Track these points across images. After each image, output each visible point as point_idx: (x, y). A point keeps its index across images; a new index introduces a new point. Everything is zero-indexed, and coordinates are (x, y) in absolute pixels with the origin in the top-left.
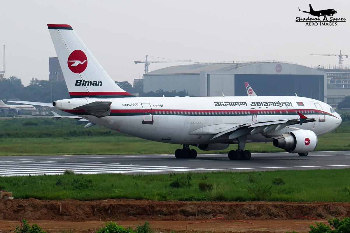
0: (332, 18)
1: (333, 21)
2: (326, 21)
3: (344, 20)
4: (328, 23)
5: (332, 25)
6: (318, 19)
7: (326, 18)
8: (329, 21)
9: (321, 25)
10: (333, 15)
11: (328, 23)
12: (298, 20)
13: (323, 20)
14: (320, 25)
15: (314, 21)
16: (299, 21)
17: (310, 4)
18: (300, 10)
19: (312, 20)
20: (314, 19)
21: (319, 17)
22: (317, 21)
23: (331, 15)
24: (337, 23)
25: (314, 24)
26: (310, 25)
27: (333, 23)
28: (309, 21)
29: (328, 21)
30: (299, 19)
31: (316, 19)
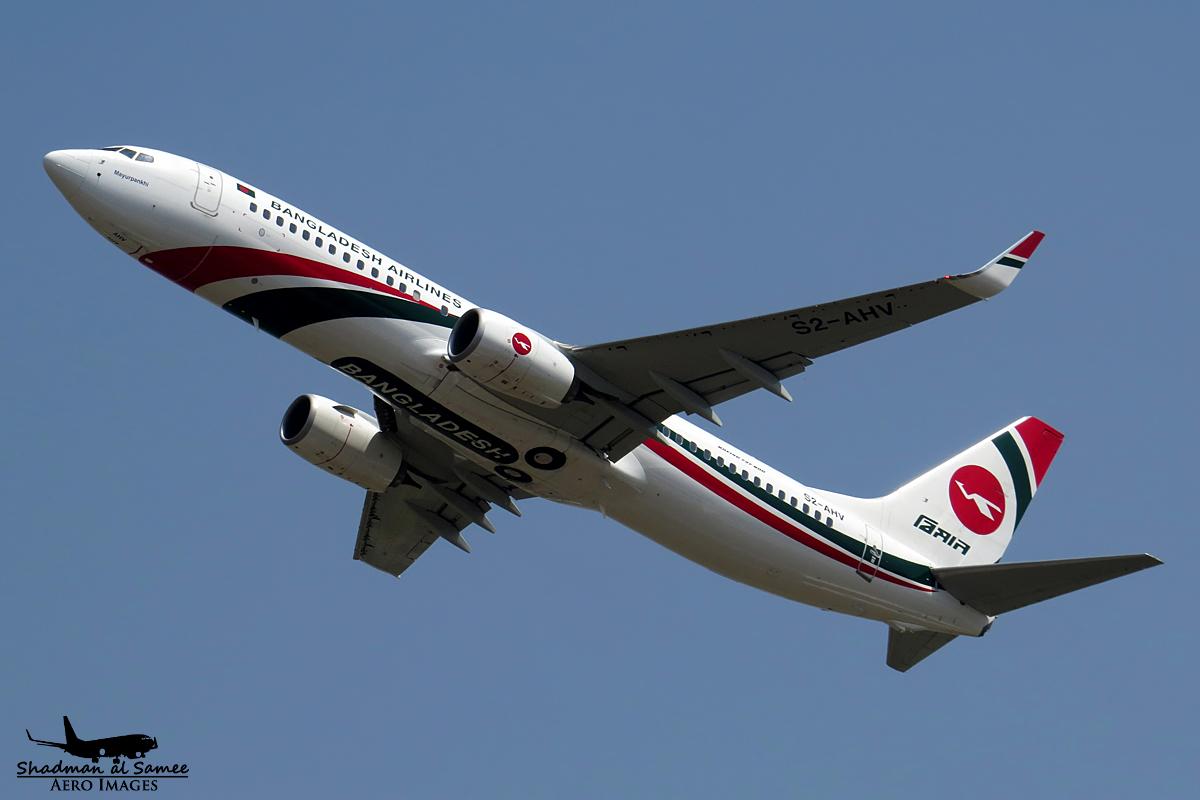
0: (142, 763)
1: (143, 774)
2: (121, 774)
3: (182, 771)
4: (128, 781)
5: (141, 787)
6: (94, 770)
7: (120, 766)
8: (131, 773)
9: (105, 785)
10: (143, 756)
11: (128, 781)
12: (26, 770)
13: (112, 772)
14: (101, 789)
15: (81, 774)
16: (27, 774)
17: (66, 720)
18: (31, 739)
19: (73, 772)
20: (80, 769)
21: (95, 760)
22: (91, 774)
23: (138, 754)
24: (160, 782)
25: (79, 786)
26: (67, 788)
27: (144, 782)
28: (64, 774)
29: (128, 774)
30: (27, 767)
31: (86, 768)
